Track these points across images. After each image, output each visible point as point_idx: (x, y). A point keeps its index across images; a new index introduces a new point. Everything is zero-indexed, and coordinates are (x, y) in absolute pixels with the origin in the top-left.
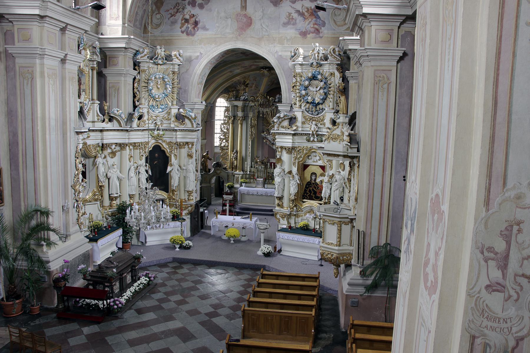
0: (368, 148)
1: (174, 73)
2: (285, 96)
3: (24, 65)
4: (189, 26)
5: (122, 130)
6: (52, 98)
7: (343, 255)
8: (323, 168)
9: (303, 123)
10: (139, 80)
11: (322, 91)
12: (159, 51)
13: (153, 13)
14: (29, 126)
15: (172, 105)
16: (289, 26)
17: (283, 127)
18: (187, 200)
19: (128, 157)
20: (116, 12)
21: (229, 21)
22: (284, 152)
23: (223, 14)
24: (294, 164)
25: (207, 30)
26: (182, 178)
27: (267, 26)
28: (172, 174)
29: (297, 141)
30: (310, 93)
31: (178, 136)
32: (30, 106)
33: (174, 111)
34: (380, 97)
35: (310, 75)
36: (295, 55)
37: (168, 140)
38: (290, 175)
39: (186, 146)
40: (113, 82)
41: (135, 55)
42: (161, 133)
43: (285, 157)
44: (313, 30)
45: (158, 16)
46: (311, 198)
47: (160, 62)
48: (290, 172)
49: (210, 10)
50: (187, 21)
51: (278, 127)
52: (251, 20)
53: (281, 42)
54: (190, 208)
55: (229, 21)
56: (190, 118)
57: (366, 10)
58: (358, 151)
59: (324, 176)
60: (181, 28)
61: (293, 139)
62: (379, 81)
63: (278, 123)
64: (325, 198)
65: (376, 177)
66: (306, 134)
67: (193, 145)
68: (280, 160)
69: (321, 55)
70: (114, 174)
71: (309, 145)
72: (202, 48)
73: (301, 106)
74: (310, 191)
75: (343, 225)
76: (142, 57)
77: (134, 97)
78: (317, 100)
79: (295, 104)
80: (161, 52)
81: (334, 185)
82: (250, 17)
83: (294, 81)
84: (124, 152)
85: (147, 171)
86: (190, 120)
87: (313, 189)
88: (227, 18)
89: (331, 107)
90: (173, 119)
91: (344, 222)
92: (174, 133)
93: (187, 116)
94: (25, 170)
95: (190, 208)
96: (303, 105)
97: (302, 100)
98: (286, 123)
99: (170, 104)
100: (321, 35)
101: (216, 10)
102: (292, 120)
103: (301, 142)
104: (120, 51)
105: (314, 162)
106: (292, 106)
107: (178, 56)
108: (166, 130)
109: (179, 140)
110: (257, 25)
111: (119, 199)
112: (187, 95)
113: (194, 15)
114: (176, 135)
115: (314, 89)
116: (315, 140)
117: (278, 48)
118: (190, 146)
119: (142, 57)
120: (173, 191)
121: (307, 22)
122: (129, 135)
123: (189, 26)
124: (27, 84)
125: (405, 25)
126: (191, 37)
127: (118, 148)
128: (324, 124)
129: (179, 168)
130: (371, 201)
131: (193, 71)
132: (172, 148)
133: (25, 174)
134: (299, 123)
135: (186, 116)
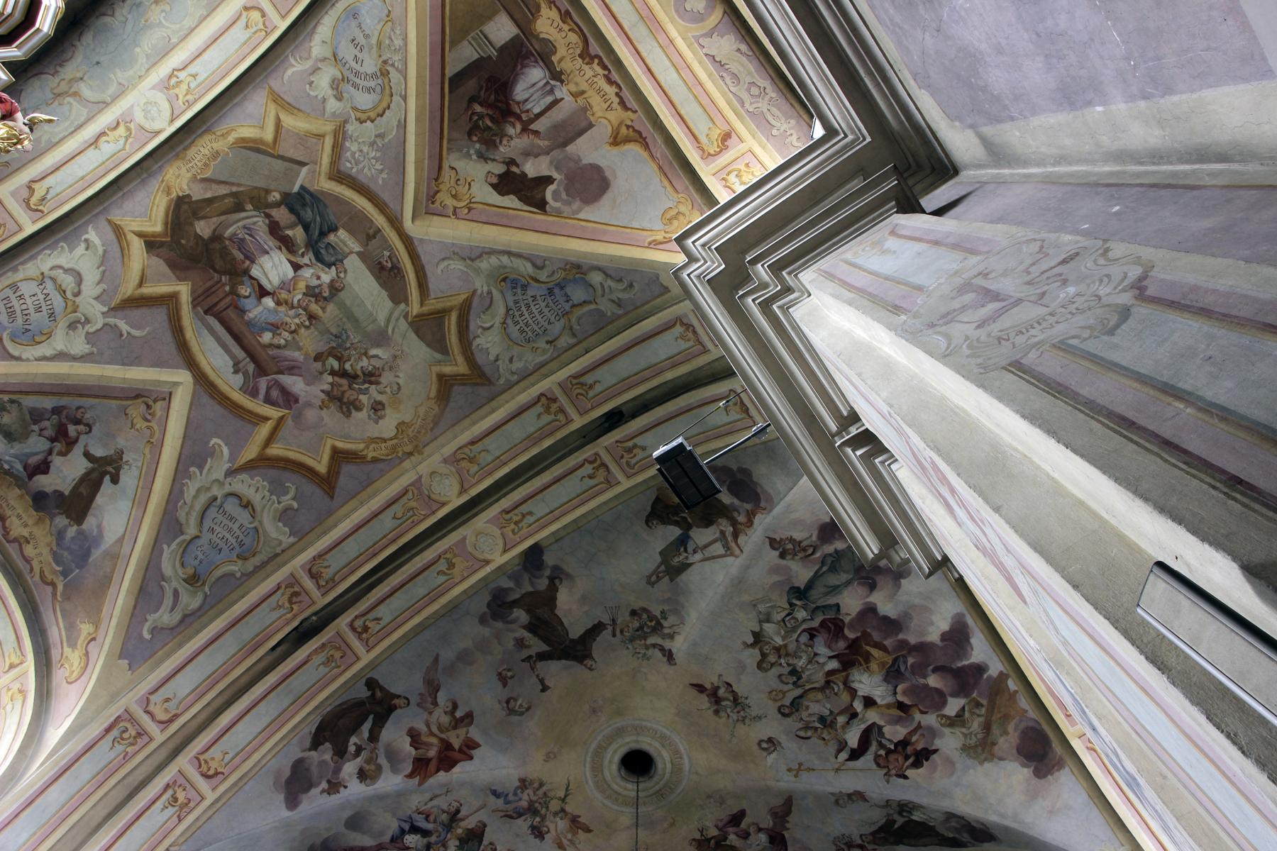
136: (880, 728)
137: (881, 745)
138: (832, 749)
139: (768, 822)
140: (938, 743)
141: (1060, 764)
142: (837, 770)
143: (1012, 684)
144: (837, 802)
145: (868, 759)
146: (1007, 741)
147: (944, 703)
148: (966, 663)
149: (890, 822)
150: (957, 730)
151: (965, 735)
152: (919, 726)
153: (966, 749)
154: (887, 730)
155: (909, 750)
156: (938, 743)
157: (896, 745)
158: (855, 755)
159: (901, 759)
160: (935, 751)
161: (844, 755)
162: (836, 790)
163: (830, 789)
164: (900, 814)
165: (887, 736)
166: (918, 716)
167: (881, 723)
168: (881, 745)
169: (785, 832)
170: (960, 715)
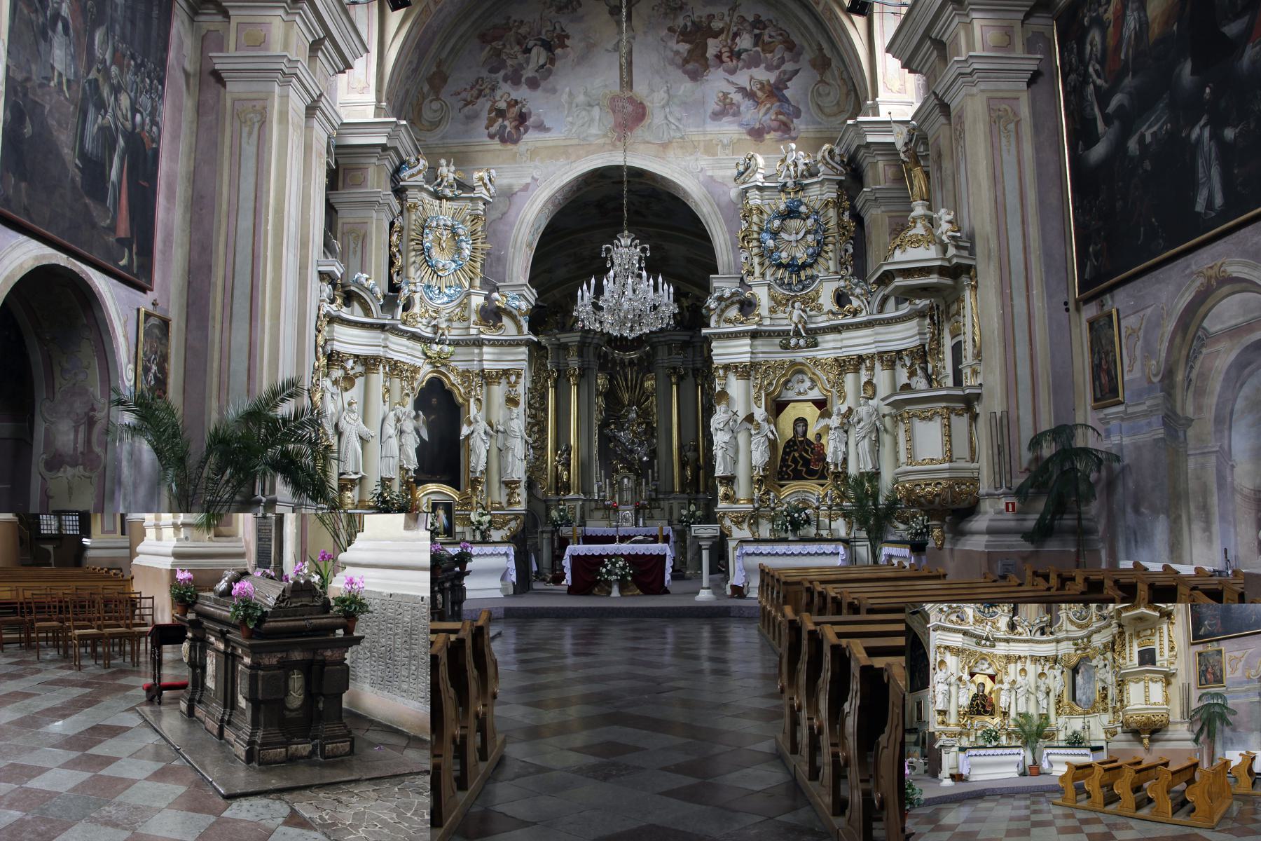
0: (993, 244)
1: (476, 218)
2: (725, 258)
3: (244, 96)
4: (507, 123)
6: (295, 174)
7: (959, 481)
8: (820, 404)
9: (772, 310)
10: (402, 228)
11: (810, 238)
12: (443, 170)
13: (424, 99)
14: (245, 223)
15: (471, 286)
16: (725, 119)
17: (729, 321)
18: (505, 504)
19: (381, 390)
20: (363, 78)
21: (596, 112)
22: (732, 378)
23: (581, 98)
24: (758, 398)
25: (547, 130)
26: (494, 451)
27: (679, 120)
28: (471, 442)
29: (760, 349)
30: (782, 246)
31: (485, 357)
32: (252, 180)
33: (477, 301)
34: (1004, 148)
35: (782, 207)
36: (746, 169)
37: (461, 367)
38: (749, 426)
39: (503, 381)
40: (352, 221)
41: (397, 171)
42: (447, 349)
43: (736, 387)
44: (775, 124)
45: (436, 105)
46: (798, 476)
47: (448, 192)
48: (750, 418)
50: (501, 113)
51: (718, 322)
53: (710, 149)
54: (513, 524)
55: (596, 112)
56: (515, 312)
59: (830, 416)
60: (487, 128)
61: (751, 346)
62: (1000, 117)
63: (718, 311)
65: (1016, 302)
66: (779, 334)
67: (518, 376)
68: (724, 394)
69: (801, 167)
70: (353, 426)
71: (788, 356)
72: (536, 167)
73: (763, 275)
74: (795, 461)
75: (953, 416)
76: (412, 176)
77: (391, 264)
78: (801, 256)
79: (750, 273)
80: (448, 172)
81: (852, 432)
82: (641, 103)
83: (744, 225)
84: (374, 377)
85: (417, 431)
86: (513, 318)
87: (801, 456)
88: (590, 105)
89: (832, 269)
90: (474, 318)
91: (954, 409)
92: (476, 351)
94: (226, 325)
95: (513, 524)
96: (769, 273)
97: (767, 263)
98: (733, 312)
99: (467, 285)
100: (793, 134)
101: (567, 89)
102: (747, 306)
103: (769, 351)
104: (370, 155)
105: (799, 393)
106: (742, 279)
107: (487, 181)
108: (455, 343)
109: (487, 365)
110: (656, 118)
111: (357, 488)
112: (504, 268)
113: (516, 102)
114: (481, 354)
115: (793, 238)
116: (802, 342)
117: (704, 162)
118: (513, 378)
119: (412, 176)
120: (475, 483)
121: (763, 110)
122: (386, 339)
123: (507, 123)
124: (250, 134)
125: (1032, 20)
126: (510, 147)
127: (359, 369)
128: (819, 308)
129: (488, 428)
131: (517, 215)
132: (470, 385)
133: (226, 334)
135: (504, 310)
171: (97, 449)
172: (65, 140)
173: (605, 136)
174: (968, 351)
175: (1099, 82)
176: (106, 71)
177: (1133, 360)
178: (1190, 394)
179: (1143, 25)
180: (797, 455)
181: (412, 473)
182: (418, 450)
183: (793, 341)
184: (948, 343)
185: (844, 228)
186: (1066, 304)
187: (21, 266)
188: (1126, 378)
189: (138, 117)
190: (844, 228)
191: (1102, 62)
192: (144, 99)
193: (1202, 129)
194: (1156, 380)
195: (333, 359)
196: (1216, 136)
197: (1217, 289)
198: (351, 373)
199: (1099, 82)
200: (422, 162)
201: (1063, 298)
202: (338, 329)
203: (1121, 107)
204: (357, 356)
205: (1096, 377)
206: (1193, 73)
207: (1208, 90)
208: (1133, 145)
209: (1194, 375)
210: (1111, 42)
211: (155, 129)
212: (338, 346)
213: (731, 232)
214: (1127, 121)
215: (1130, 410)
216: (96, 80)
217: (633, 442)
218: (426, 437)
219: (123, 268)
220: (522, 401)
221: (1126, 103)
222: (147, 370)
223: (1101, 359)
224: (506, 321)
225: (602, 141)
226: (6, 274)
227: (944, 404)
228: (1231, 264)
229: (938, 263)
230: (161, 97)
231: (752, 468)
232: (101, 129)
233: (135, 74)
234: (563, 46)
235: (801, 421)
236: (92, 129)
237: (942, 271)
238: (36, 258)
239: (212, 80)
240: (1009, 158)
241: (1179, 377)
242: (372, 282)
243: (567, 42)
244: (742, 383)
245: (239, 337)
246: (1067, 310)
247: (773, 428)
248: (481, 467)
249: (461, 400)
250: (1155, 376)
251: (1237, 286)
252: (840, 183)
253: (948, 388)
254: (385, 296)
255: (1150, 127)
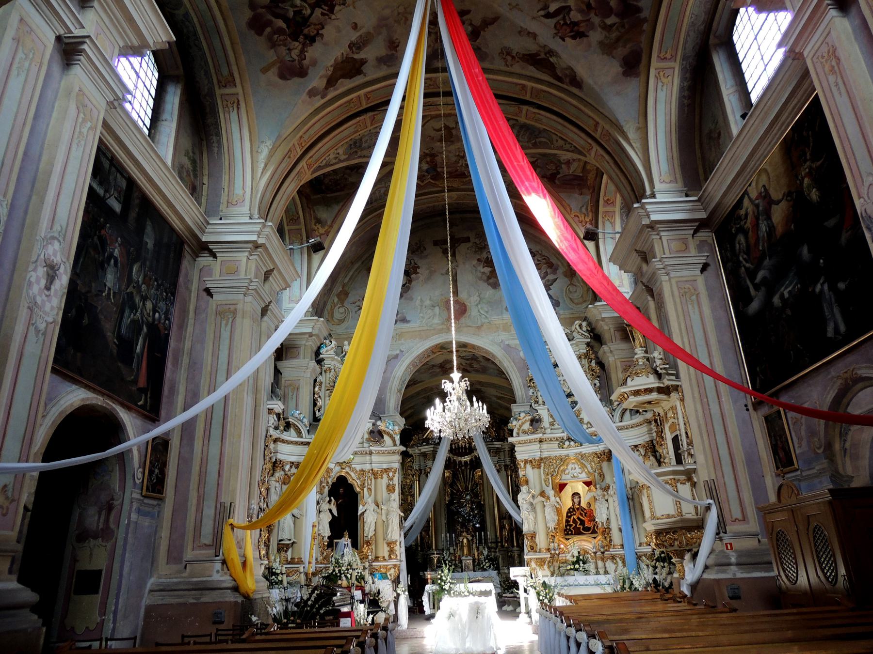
3: (224, 303)
5: (302, 443)
17: (525, 432)
18: (387, 557)
21: (437, 310)
22: (528, 466)
23: (428, 303)
25: (408, 322)
27: (487, 312)
32: (226, 352)
37: (358, 468)
39: (385, 476)
45: (342, 310)
46: (578, 533)
49: (411, 299)
52: (465, 306)
55: (437, 310)
56: (391, 432)
57: (654, 217)
58: (677, 376)
62: (686, 293)
64: (603, 523)
67: (395, 472)
77: (315, 404)
85: (330, 511)
87: (578, 518)
91: (679, 480)
92: (368, 458)
93: (387, 430)
94: (206, 442)
110: (473, 312)
111: (290, 550)
118: (391, 474)
120: (368, 543)
124: (226, 325)
125: (699, 234)
127: (294, 470)
130: (712, 438)
133: (205, 448)
134: (546, 423)
136: (571, 10)
137: (564, 19)
138: (540, 6)
139: (477, 22)
140: (591, 33)
141: (637, 75)
142: (534, 18)
143: (645, 26)
144: (520, 32)
145: (552, 22)
146: (622, 51)
147: (608, 16)
148: (635, 3)
149: (537, 54)
150: (604, 33)
151: (606, 36)
152: (588, 20)
153: (601, 43)
154: (572, 13)
155: (576, 28)
156: (591, 33)
157: (571, 22)
158: (548, 16)
159: (568, 30)
160: (587, 36)
161: (542, 13)
162: (525, 27)
163: (522, 25)
164: (546, 54)
165: (571, 16)
166: (592, 15)
167: (573, 8)
168: (564, 19)
169: (482, 33)
170: (611, 26)
171: (112, 526)
172: (108, 327)
173: (443, 324)
174: (684, 441)
175: (747, 265)
176: (139, 287)
177: (800, 439)
178: (847, 459)
179: (771, 228)
180: (575, 517)
181: (326, 539)
182: (330, 523)
183: (567, 443)
184: (669, 436)
185: (593, 370)
186: (746, 406)
187: (72, 405)
188: (797, 452)
189: (157, 315)
190: (593, 370)
191: (748, 252)
192: (162, 304)
193: (822, 285)
194: (820, 451)
195: (276, 465)
196: (833, 288)
197: (853, 386)
198: (289, 473)
199: (747, 265)
200: (334, 342)
201: (744, 402)
202: (281, 447)
203: (764, 278)
204: (293, 463)
205: (775, 452)
206: (809, 251)
207: (821, 261)
208: (776, 300)
209: (847, 445)
210: (752, 241)
211: (167, 322)
212: (279, 456)
213: (522, 377)
214: (770, 286)
215: (804, 474)
216: (132, 293)
217: (470, 515)
218: (336, 514)
219: (141, 407)
220: (397, 488)
221: (767, 275)
222: (151, 472)
223: (776, 440)
224: (386, 437)
225: (441, 327)
226: (60, 410)
227: (671, 477)
228: (860, 369)
229: (657, 385)
230: (172, 303)
231: (547, 528)
232: (133, 321)
233: (157, 290)
234: (416, 273)
235: (576, 494)
236: (126, 321)
237: (660, 390)
238: (83, 400)
239: (205, 294)
240: (695, 317)
241: (837, 446)
242: (302, 416)
243: (418, 270)
244: (536, 470)
245: (214, 450)
246: (748, 410)
247: (558, 499)
248: (371, 533)
249: (358, 489)
250: (819, 448)
251: (867, 383)
252: (588, 344)
253: (673, 466)
254: (310, 425)
255: (786, 288)
